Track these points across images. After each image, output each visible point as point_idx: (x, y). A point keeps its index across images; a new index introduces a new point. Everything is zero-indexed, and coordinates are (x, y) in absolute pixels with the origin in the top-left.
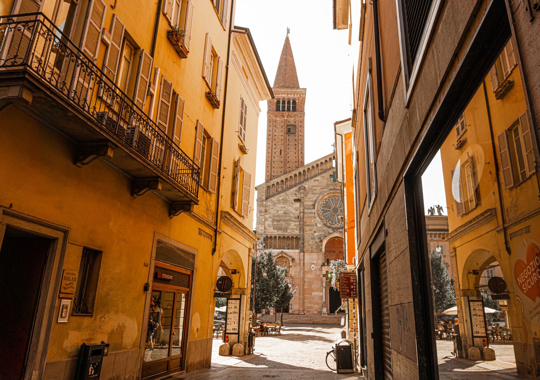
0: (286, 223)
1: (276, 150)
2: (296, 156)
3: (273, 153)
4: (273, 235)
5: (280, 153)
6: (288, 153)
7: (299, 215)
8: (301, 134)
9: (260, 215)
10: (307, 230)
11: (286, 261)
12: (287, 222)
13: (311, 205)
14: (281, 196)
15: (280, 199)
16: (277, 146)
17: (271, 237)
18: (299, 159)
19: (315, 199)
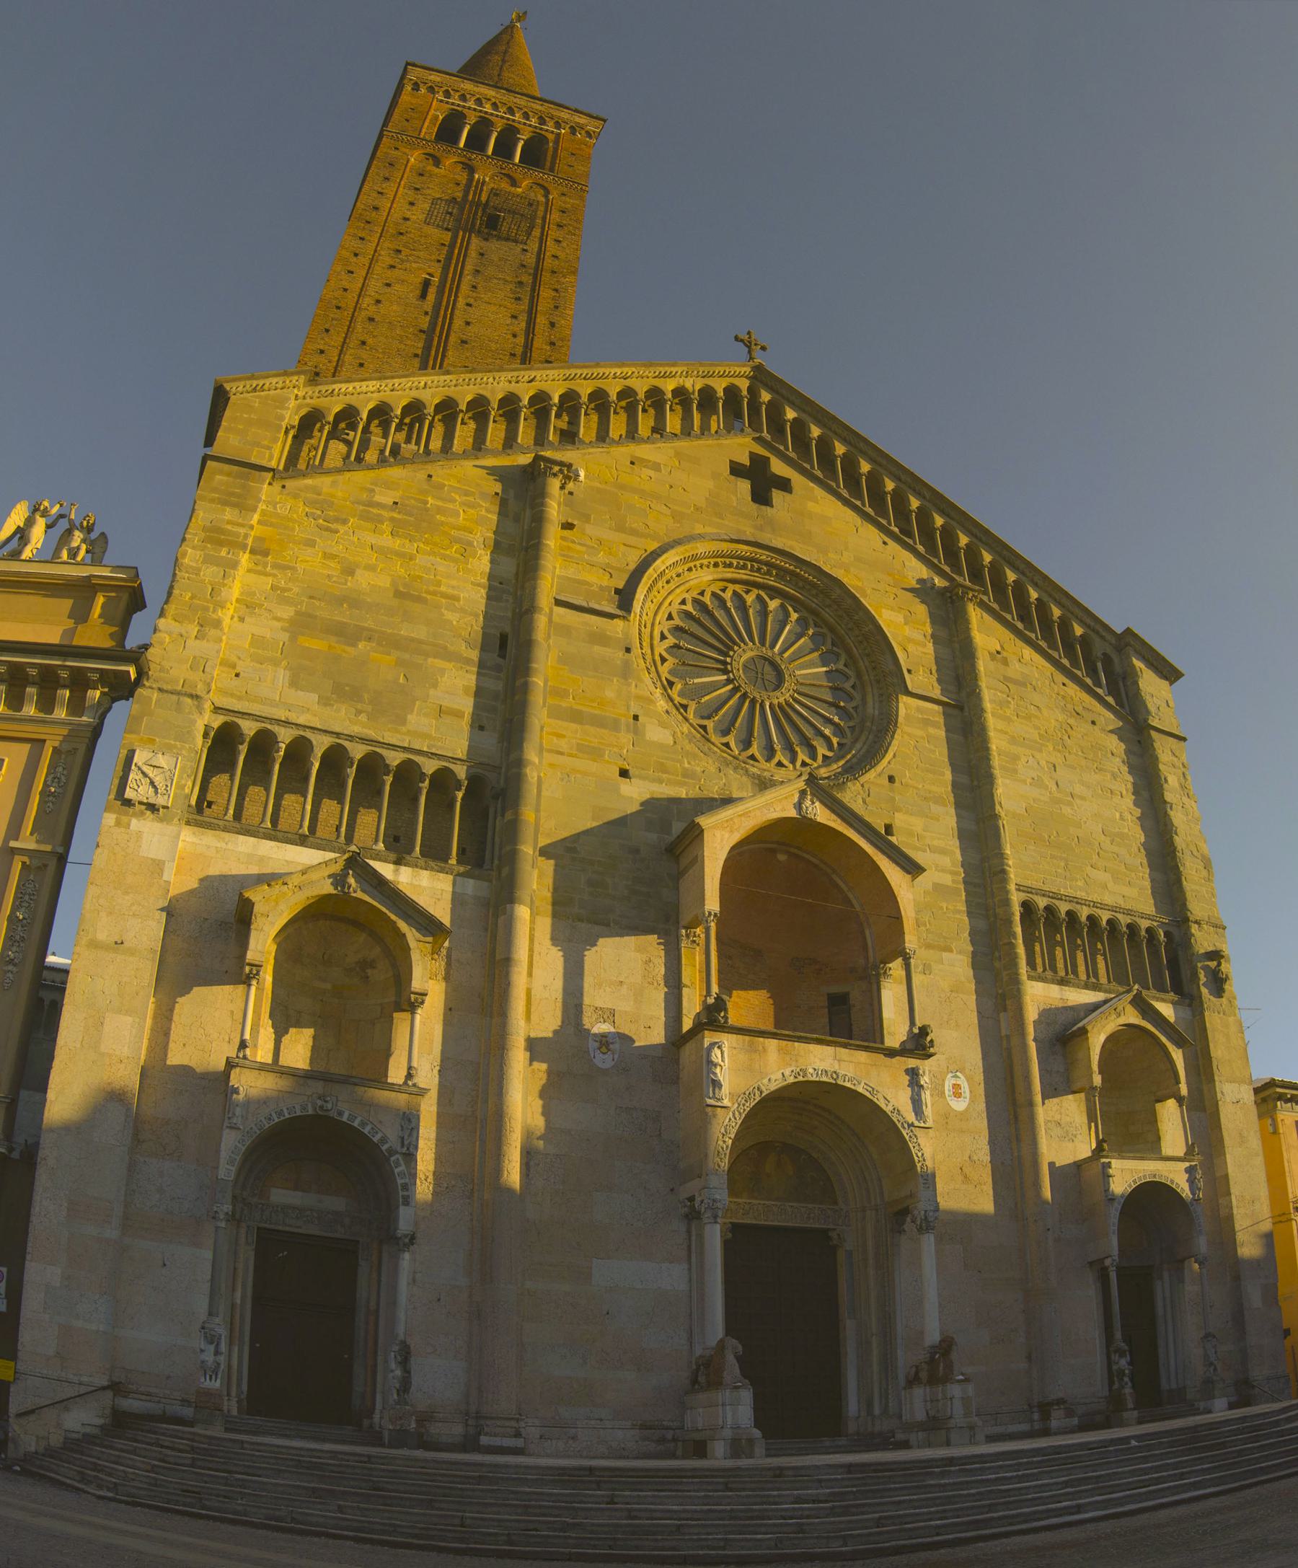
0: (400, 663)
1: (396, 273)
2: (516, 329)
3: (375, 286)
4: (287, 723)
5: (418, 292)
6: (469, 305)
7: (508, 629)
8: (561, 255)
9: (208, 560)
10: (563, 745)
11: (366, 965)
12: (407, 656)
13: (601, 588)
14: (388, 485)
15: (378, 498)
16: (402, 261)
17: (264, 743)
18: (536, 344)
19: (633, 559)
